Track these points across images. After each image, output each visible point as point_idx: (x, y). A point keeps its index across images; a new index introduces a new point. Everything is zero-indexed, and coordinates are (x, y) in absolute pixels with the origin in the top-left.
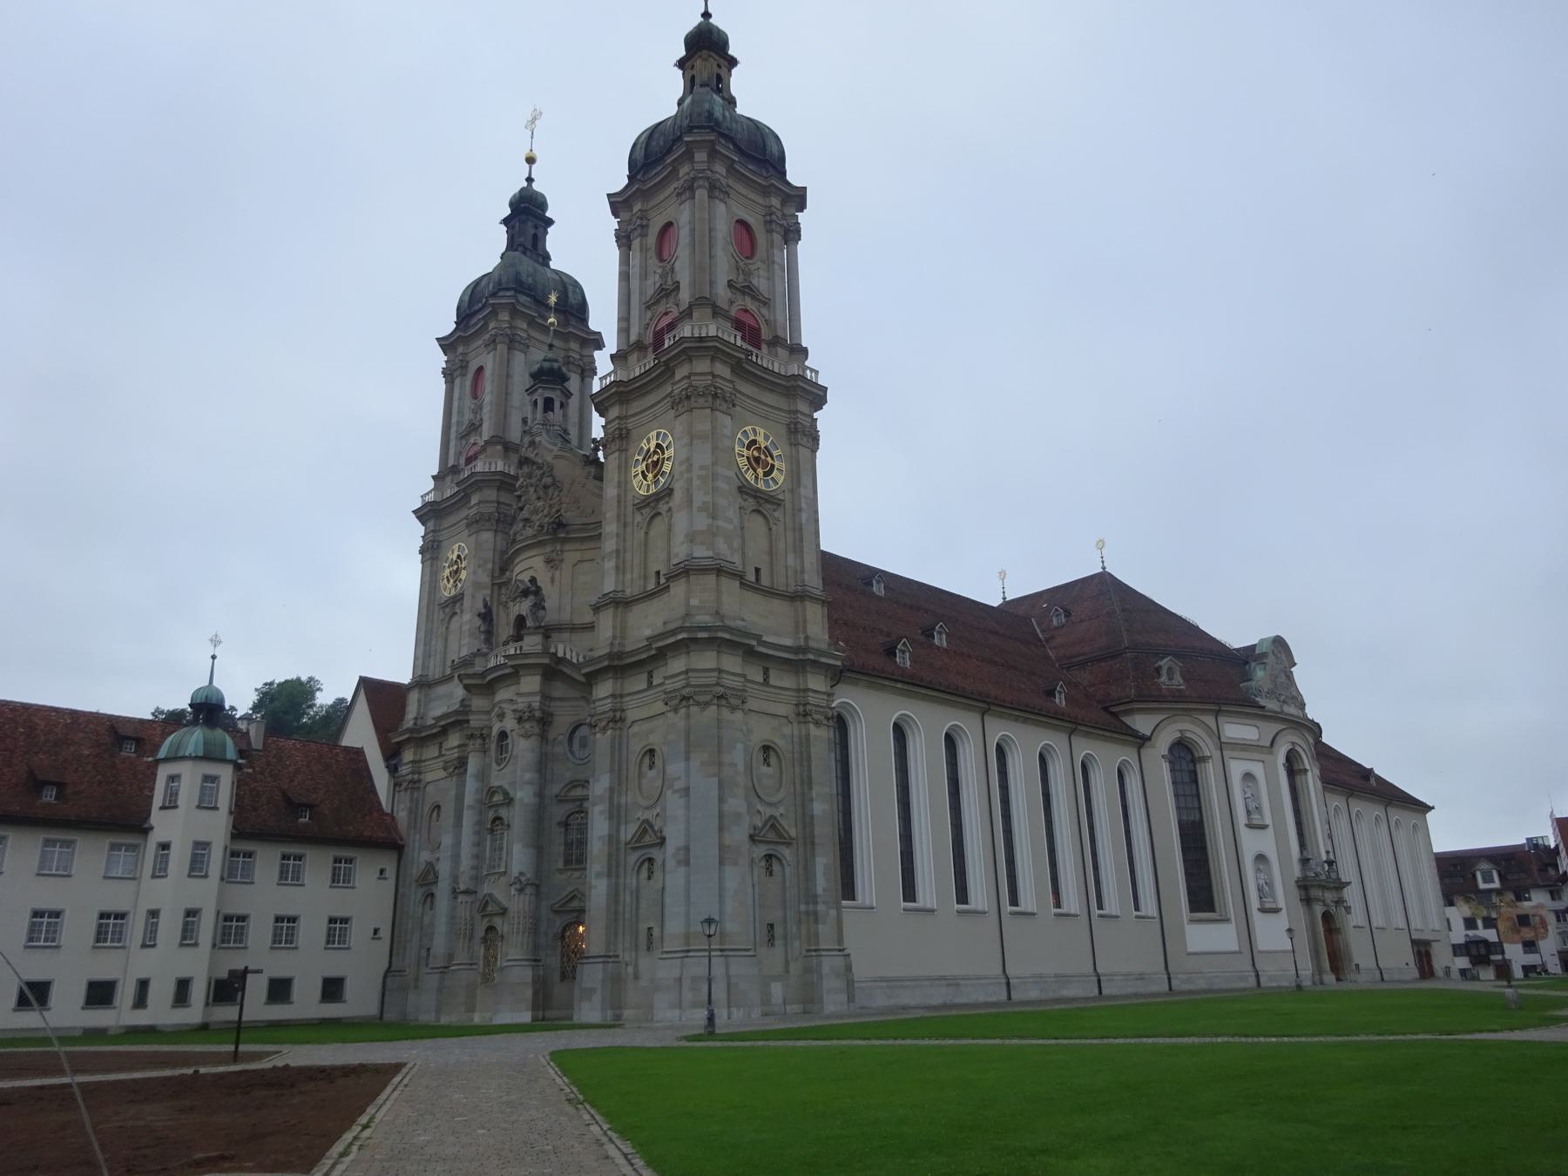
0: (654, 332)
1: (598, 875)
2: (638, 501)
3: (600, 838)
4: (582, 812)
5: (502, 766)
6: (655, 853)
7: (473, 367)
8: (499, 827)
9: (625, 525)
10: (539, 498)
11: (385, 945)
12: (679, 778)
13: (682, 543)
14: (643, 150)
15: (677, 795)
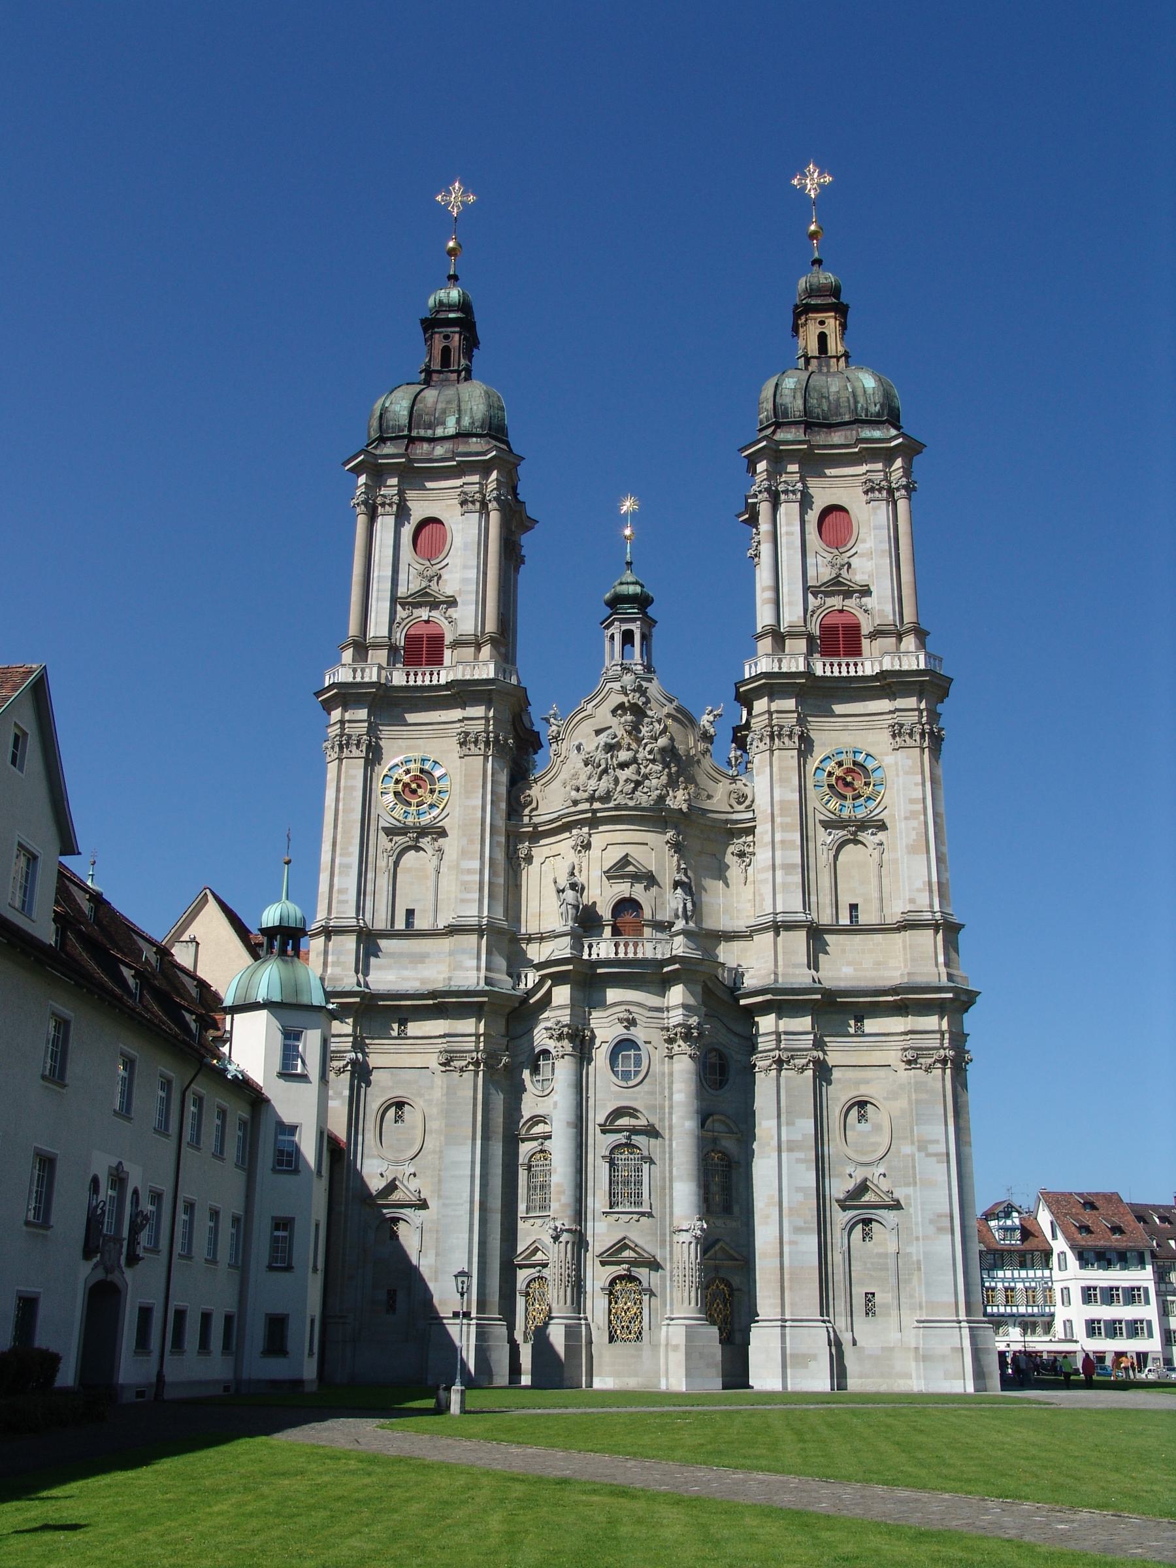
0: (820, 624)
1: (797, 1230)
2: (823, 818)
3: (799, 1189)
4: (720, 1152)
5: (631, 1083)
6: (889, 1216)
7: (419, 509)
8: (623, 1157)
9: (804, 838)
10: (653, 761)
11: (320, 1276)
12: (937, 1142)
13: (919, 890)
14: (799, 403)
15: (934, 1159)
